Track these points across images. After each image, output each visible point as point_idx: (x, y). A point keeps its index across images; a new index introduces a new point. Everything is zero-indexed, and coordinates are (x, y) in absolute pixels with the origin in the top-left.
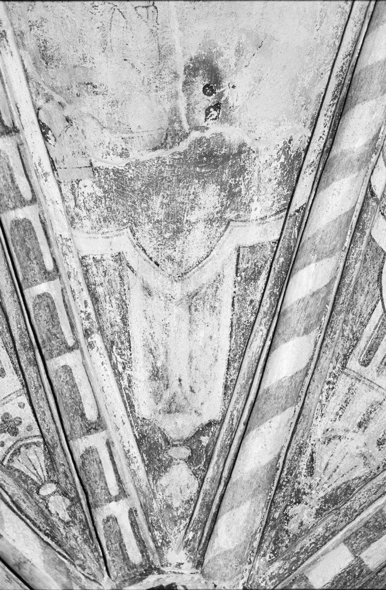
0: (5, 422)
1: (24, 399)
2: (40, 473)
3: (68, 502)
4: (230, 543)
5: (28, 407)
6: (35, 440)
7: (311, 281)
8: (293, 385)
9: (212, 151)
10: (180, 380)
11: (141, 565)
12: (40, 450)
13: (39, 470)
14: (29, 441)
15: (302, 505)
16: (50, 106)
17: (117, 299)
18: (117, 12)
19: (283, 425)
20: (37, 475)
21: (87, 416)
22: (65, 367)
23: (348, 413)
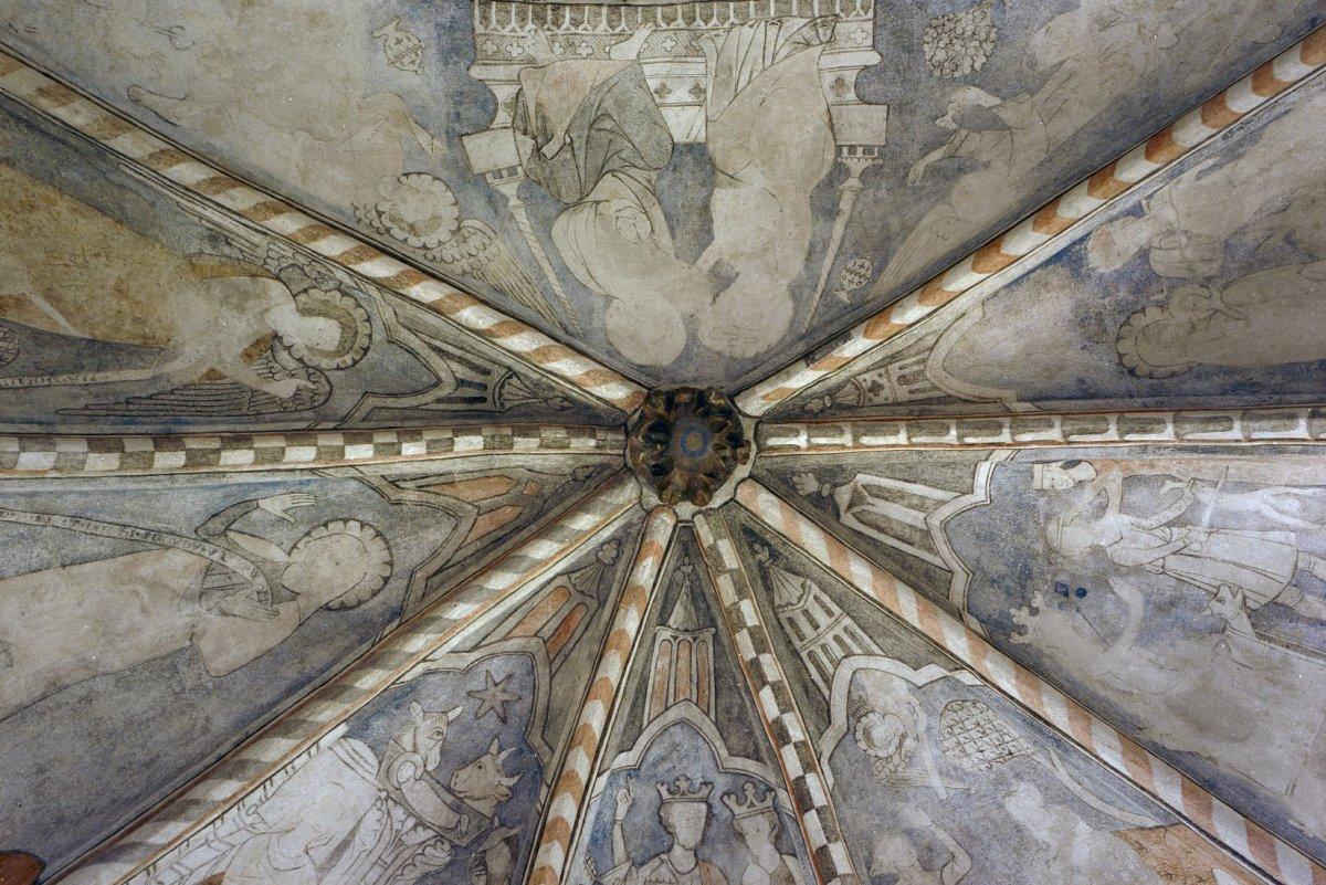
1: (890, 401)
9: (1032, 579)
12: (854, 403)
23: (817, 606)
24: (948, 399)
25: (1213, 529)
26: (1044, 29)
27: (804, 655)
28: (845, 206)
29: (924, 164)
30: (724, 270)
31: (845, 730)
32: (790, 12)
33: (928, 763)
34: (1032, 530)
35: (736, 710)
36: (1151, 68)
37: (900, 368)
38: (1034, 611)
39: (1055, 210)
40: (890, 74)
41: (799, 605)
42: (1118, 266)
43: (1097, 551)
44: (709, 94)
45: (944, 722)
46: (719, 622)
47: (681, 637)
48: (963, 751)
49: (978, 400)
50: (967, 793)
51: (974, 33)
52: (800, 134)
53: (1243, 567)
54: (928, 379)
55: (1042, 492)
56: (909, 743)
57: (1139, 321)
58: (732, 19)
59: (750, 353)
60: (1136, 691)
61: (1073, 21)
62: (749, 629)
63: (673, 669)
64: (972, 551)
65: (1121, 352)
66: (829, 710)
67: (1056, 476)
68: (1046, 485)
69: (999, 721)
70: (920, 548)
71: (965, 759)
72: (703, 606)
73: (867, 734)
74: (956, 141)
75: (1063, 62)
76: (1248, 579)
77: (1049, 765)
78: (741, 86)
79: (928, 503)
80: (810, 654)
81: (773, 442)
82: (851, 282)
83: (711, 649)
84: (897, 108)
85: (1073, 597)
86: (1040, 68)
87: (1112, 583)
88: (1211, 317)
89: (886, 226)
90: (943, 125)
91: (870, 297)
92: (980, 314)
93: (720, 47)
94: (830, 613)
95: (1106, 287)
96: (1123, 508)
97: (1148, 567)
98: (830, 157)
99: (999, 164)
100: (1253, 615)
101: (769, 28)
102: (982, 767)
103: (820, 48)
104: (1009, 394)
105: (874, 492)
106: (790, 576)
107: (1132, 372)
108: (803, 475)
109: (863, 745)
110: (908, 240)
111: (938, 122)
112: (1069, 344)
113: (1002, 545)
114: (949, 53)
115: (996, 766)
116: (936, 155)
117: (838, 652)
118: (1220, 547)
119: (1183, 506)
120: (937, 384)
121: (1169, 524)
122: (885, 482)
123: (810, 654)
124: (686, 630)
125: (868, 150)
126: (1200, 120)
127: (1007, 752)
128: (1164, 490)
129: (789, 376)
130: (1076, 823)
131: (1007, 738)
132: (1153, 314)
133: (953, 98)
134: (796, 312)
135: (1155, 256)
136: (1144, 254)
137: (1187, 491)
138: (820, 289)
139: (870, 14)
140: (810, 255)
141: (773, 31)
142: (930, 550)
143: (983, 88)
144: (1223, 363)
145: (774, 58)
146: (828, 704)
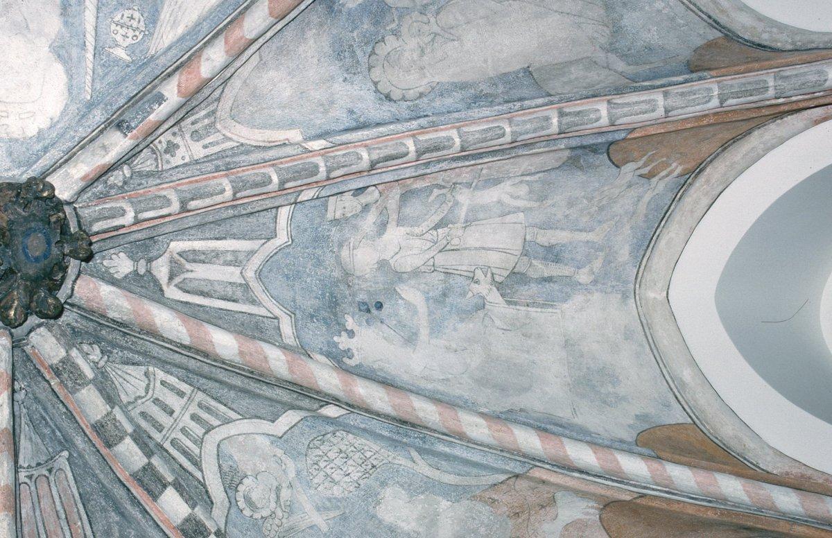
0: (174, 145)
1: (187, 160)
3: (120, 184)
4: (103, 293)
5: (181, 162)
6: (160, 166)
7: (275, 356)
8: (205, 342)
10: (192, 271)
11: (90, 230)
12: (153, 168)
14: (159, 161)
15: (100, 356)
16: (377, 194)
17: (248, 231)
18: (432, 244)
19: (179, 335)
20: (137, 164)
21: (192, 202)
22: (224, 190)
23: (166, 390)
25: (468, 223)
27: (167, 445)
31: (228, 505)
33: (308, 507)
34: (329, 260)
35: (116, 529)
38: (351, 334)
41: (148, 397)
43: (382, 265)
45: (309, 462)
46: (79, 441)
47: (36, 473)
48: (333, 481)
50: (344, 518)
53: (489, 249)
54: (219, 131)
55: (335, 222)
56: (285, 494)
57: (382, 50)
59: (32, 131)
60: (450, 376)
62: (131, 436)
63: (38, 513)
64: (287, 295)
65: (377, 80)
66: (207, 492)
67: (347, 205)
68: (337, 217)
69: (359, 442)
70: (244, 303)
71: (335, 488)
72: (47, 431)
73: (248, 500)
76: (494, 259)
77: (410, 464)
79: (241, 257)
80: (174, 443)
82: (125, 36)
83: (70, 475)
85: (374, 311)
87: (398, 290)
88: (433, 40)
94: (181, 394)
96: (400, 222)
97: (423, 269)
100: (500, 286)
102: (351, 488)
104: (295, 135)
105: (191, 257)
106: (130, 369)
107: (388, 97)
108: (114, 256)
109: (247, 512)
112: (332, 78)
113: (308, 280)
115: (361, 482)
117: (198, 430)
118: (473, 238)
119: (446, 208)
121: (436, 227)
122: (198, 245)
123: (173, 443)
124: (39, 464)
127: (370, 467)
128: (432, 198)
130: (438, 503)
131: (368, 454)
132: (390, 39)
137: (449, 195)
138: (90, 48)
142: (253, 302)
144: (456, 80)
146: (204, 485)
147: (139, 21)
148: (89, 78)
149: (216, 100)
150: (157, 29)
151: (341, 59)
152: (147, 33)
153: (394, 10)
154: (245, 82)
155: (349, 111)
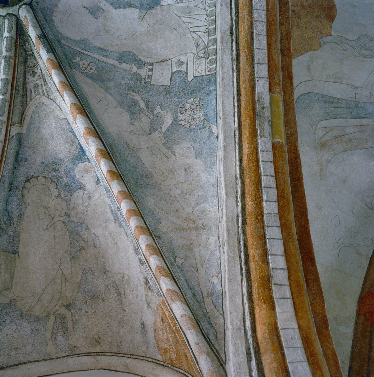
1: (27, 81)
2: (30, 58)
6: (28, 68)
11: (6, 18)
13: (30, 59)
14: (30, 68)
20: (31, 58)
24: (24, 104)
26: (190, 146)
28: (124, 65)
29: (139, 100)
30: (100, 13)
32: (210, 36)
36: (162, 187)
37: (41, 84)
39: (93, 136)
40: (183, 86)
42: (77, 177)
44: (181, 4)
49: (23, 117)
51: (194, 119)
52: (160, 47)
54: (35, 96)
57: (52, 186)
58: (209, 10)
59: (54, 19)
61: (191, 157)
65: (39, 178)
74: (148, 113)
75: (175, 155)
78: (183, 19)
81: (6, 21)
82: (84, 64)
84: (168, 90)
86: (174, 147)
88: (50, 215)
89: (109, 80)
90: (157, 108)
91: (74, 70)
92: (62, 118)
93: (199, 6)
95: (69, 173)
98: (149, 60)
99: (132, 128)
101: (205, 27)
103: (196, 53)
110: (100, 88)
111: (159, 107)
112: (46, 157)
114: (188, 110)
116: (142, 104)
120: (32, 101)
125: (150, 77)
126: (120, 190)
129: (34, 27)
132: (56, 192)
133: (169, 113)
134: (72, 40)
135: (81, 192)
136: (82, 187)
138: (83, 51)
139: (208, 73)
140: (102, 49)
141: (203, 29)
143: (171, 125)
144: (25, 216)
145: (193, 32)
147: (89, 71)
148: (70, 46)
149: (48, 96)
150: (84, 76)
151: (53, 163)
152: (83, 72)
153: (70, 197)
154: (53, 111)
155: (27, 159)
